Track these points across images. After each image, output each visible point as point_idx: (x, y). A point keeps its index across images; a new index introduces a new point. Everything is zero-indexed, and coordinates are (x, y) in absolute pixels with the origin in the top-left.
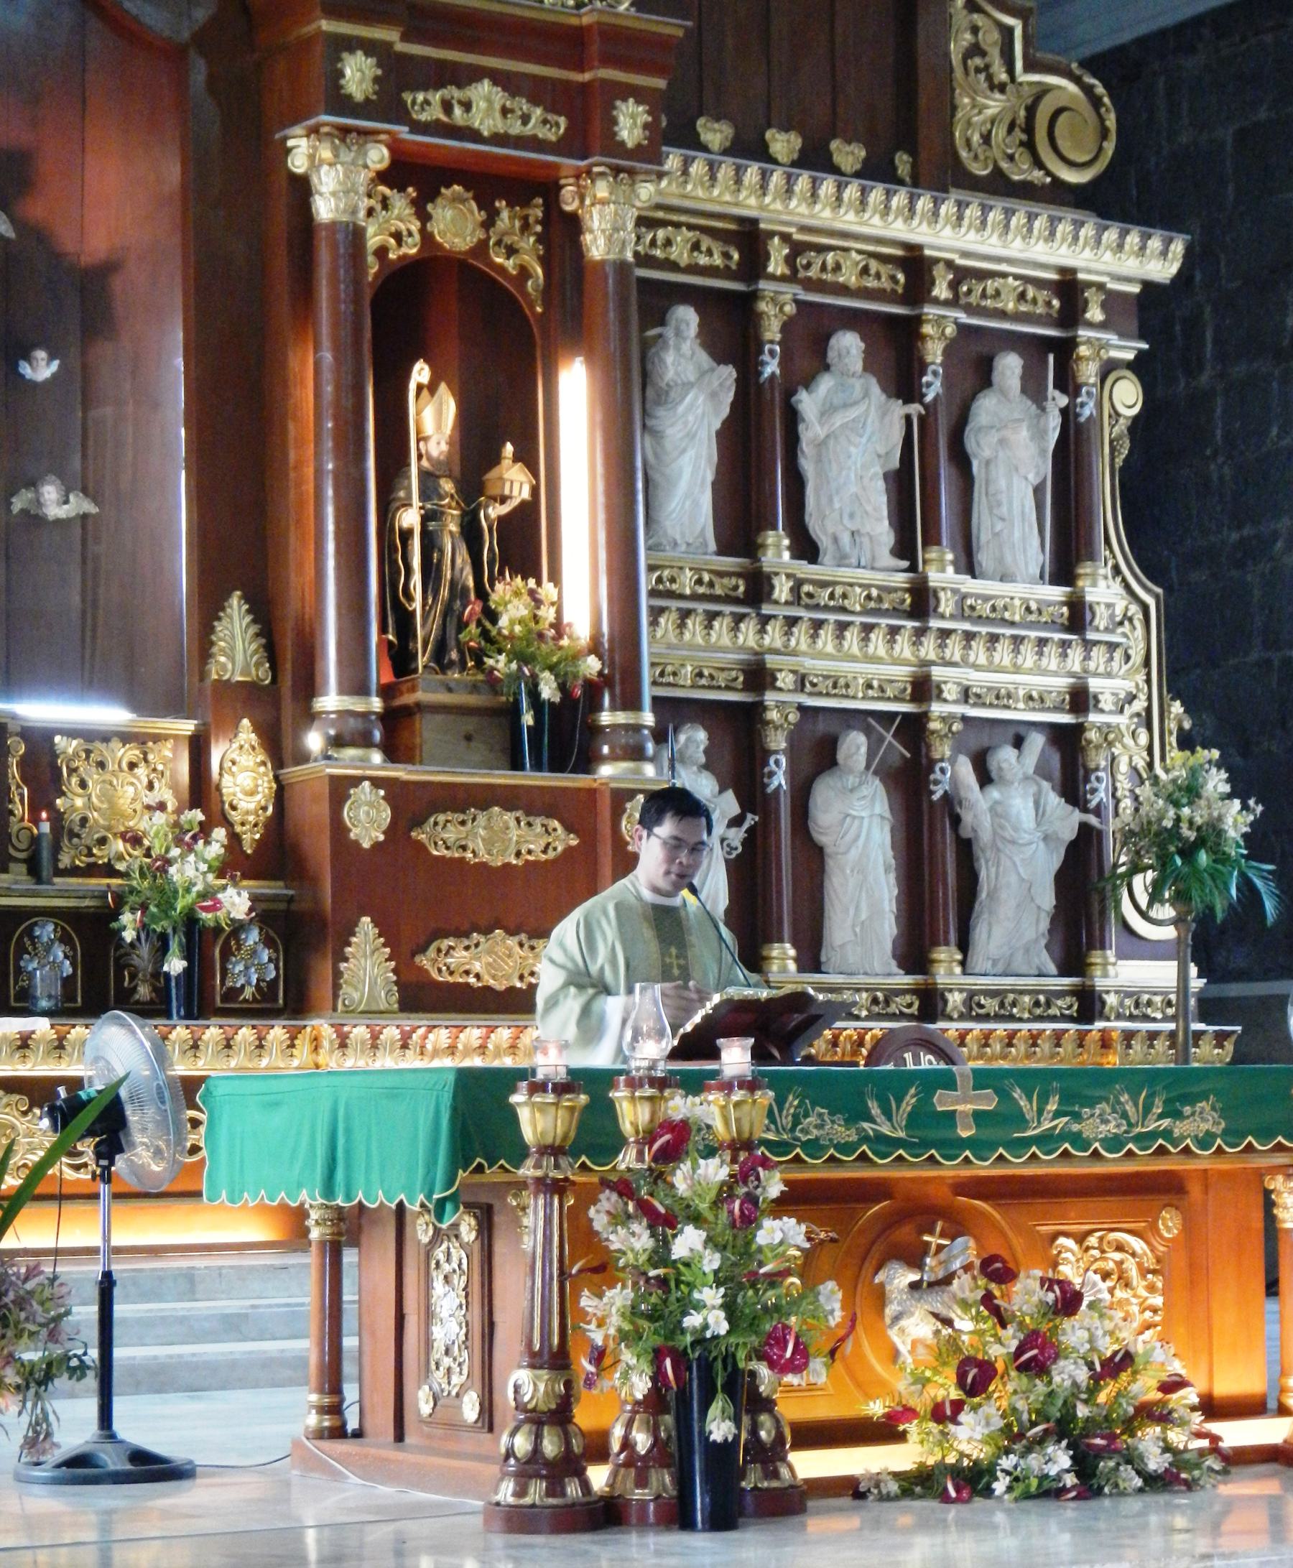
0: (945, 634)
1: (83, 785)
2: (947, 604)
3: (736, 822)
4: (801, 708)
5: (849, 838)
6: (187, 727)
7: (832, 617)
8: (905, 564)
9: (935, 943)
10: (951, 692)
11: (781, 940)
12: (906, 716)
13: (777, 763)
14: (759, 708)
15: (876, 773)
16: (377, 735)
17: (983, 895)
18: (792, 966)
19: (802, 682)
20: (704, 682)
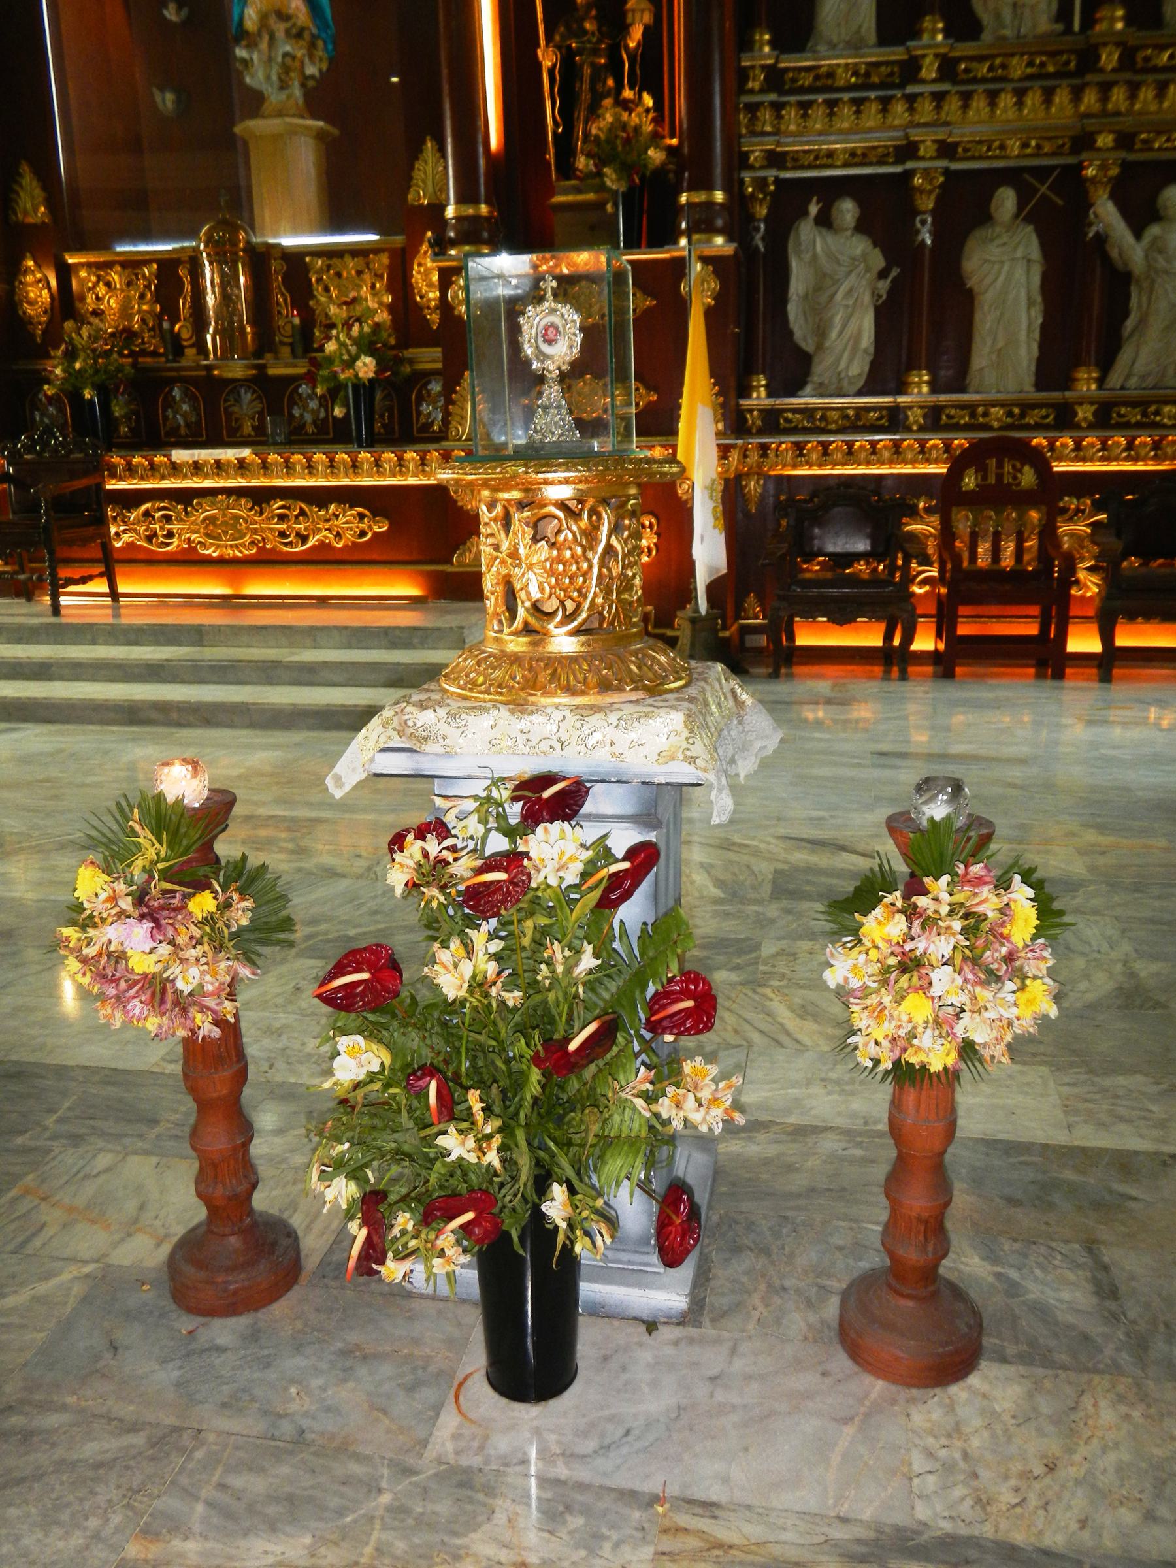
0: (1105, 89)
1: (327, 289)
2: (1109, 58)
3: (883, 275)
4: (947, 172)
5: (987, 281)
6: (399, 240)
7: (980, 88)
8: (1059, 27)
9: (1078, 363)
10: (1105, 140)
11: (920, 369)
12: (1066, 168)
13: (923, 222)
14: (909, 175)
15: (1028, 220)
16: (486, 235)
17: (1130, 323)
18: (925, 389)
19: (946, 150)
20: (856, 160)
